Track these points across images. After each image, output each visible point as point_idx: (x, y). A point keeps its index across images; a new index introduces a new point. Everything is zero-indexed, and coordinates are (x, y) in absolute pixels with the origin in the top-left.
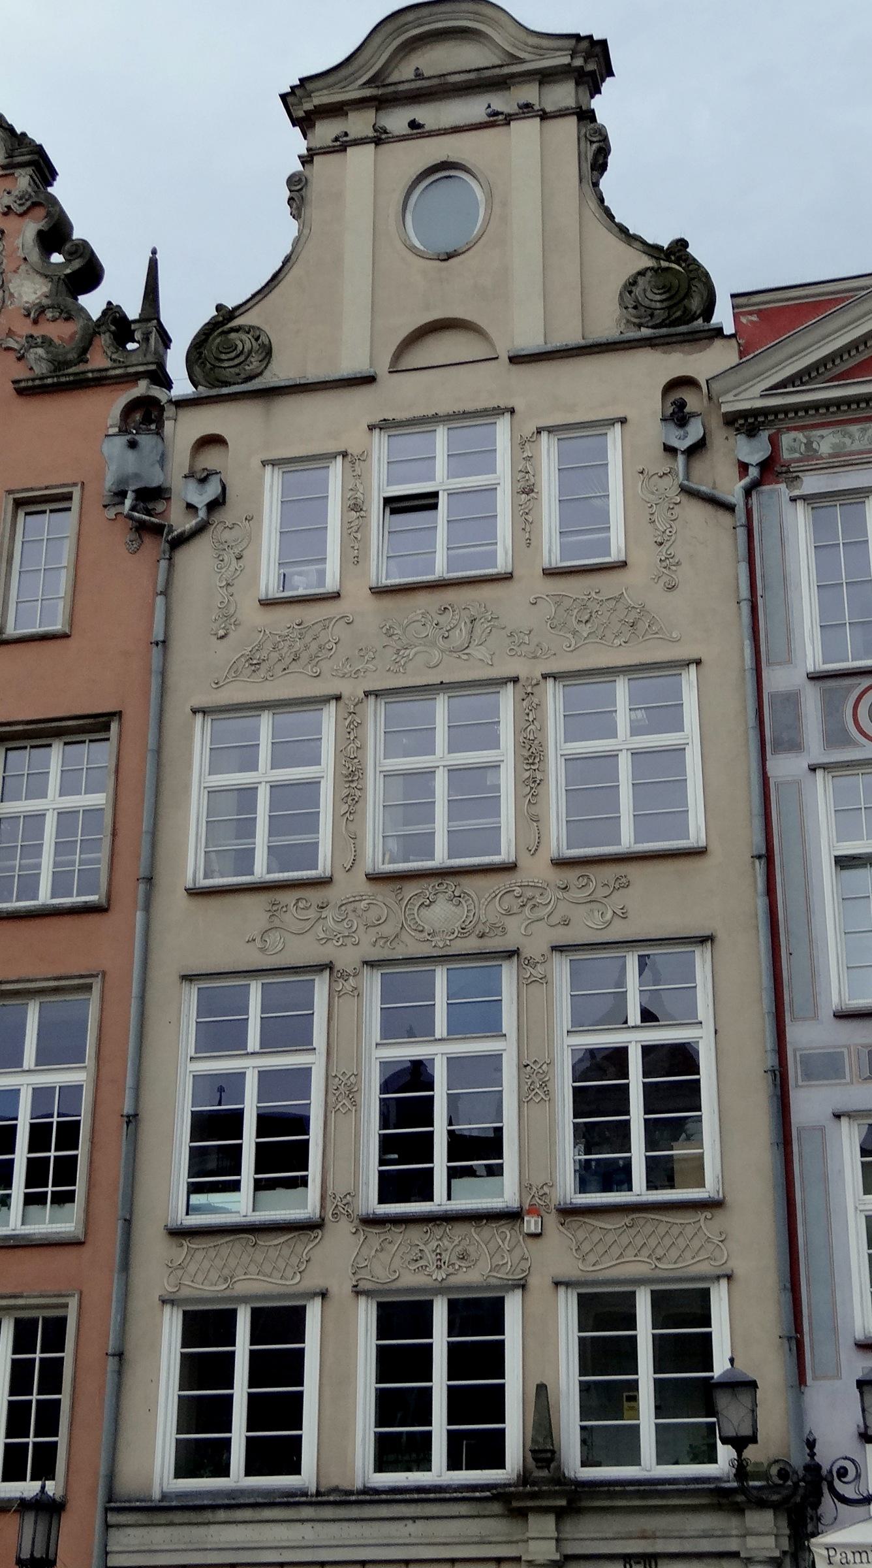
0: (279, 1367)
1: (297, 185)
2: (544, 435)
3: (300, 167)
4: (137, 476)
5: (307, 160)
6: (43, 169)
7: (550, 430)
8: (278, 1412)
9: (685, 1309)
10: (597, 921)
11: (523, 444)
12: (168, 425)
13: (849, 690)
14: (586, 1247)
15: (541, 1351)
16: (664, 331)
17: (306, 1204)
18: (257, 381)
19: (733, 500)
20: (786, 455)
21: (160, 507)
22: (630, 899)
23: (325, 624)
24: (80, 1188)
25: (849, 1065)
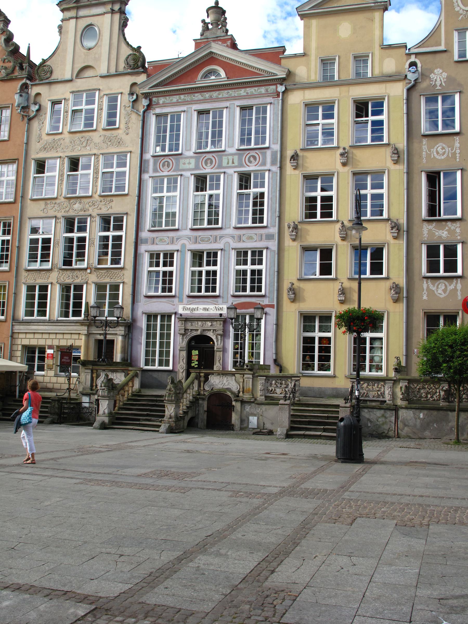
0: (43, 297)
1: (60, 27)
2: (105, 96)
3: (61, 23)
5: (63, 21)
6: (7, 22)
7: (106, 95)
8: (43, 305)
9: (115, 288)
10: (106, 209)
11: (100, 98)
12: (30, 90)
13: (159, 159)
14: (99, 276)
15: (89, 296)
16: (133, 70)
17: (48, 266)
18: (50, 79)
19: (140, 114)
20: (153, 103)
21: (27, 110)
22: (113, 204)
23: (59, 140)
24: (9, 260)
25: (149, 241)
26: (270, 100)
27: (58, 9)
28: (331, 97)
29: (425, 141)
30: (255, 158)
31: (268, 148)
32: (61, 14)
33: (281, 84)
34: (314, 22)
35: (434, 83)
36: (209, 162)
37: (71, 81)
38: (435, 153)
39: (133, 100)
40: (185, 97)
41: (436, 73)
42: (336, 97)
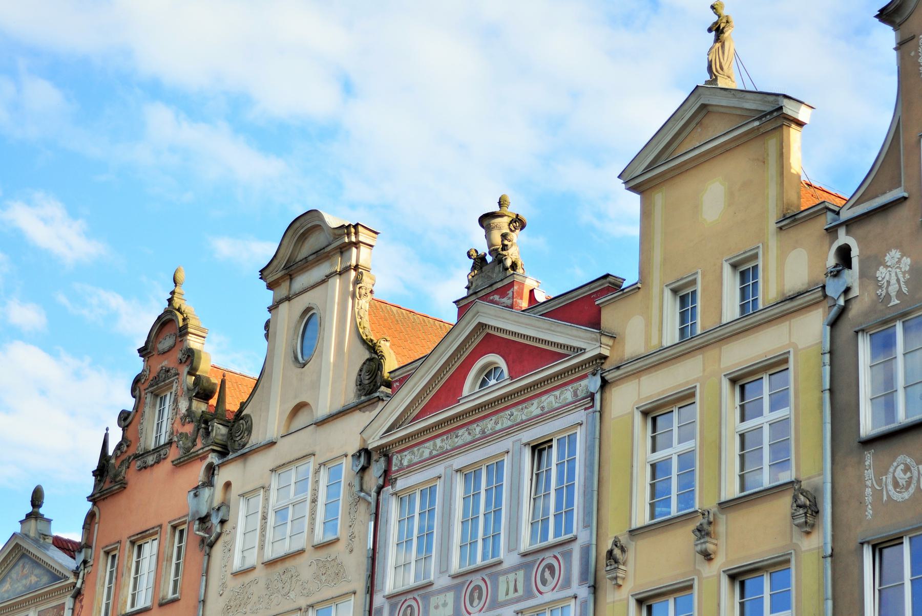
3: (268, 316)
4: (197, 512)
26: (580, 415)
27: (263, 284)
28: (687, 383)
29: (869, 458)
30: (551, 568)
31: (574, 539)
32: (271, 292)
33: (594, 374)
34: (659, 198)
35: (884, 293)
36: (476, 595)
37: (272, 444)
38: (891, 487)
39: (360, 467)
40: (443, 441)
41: (889, 264)
42: (697, 380)
